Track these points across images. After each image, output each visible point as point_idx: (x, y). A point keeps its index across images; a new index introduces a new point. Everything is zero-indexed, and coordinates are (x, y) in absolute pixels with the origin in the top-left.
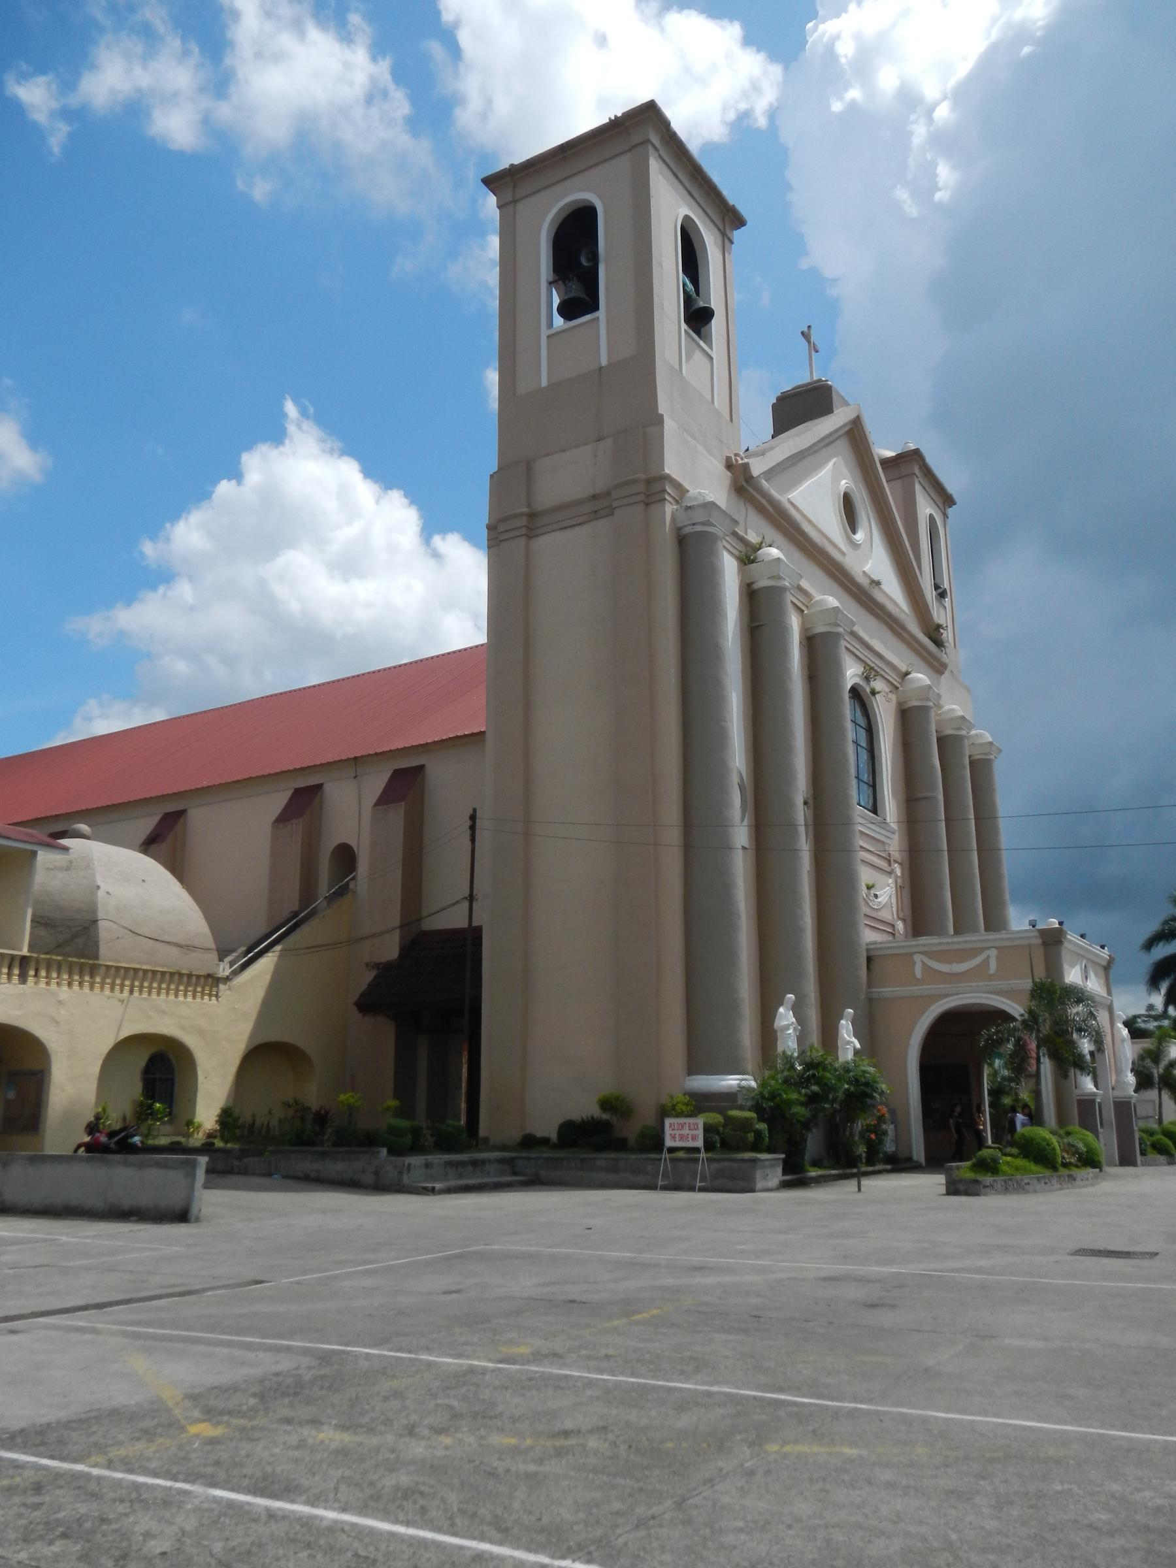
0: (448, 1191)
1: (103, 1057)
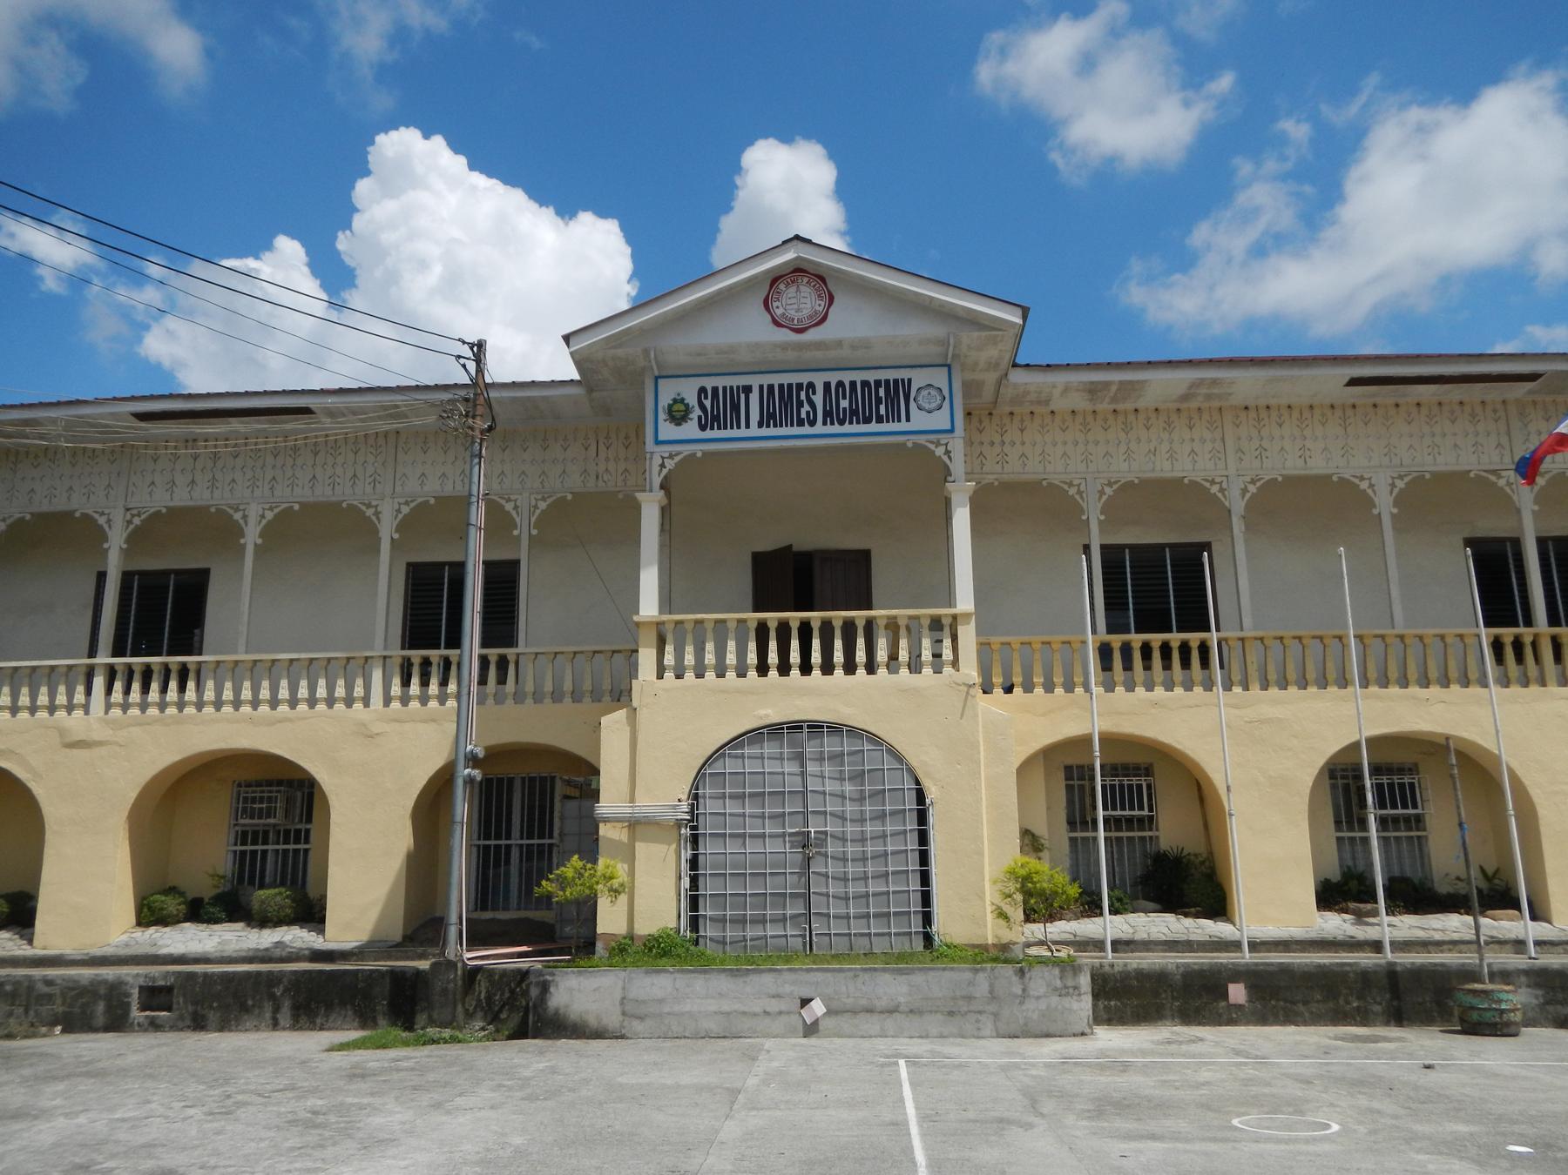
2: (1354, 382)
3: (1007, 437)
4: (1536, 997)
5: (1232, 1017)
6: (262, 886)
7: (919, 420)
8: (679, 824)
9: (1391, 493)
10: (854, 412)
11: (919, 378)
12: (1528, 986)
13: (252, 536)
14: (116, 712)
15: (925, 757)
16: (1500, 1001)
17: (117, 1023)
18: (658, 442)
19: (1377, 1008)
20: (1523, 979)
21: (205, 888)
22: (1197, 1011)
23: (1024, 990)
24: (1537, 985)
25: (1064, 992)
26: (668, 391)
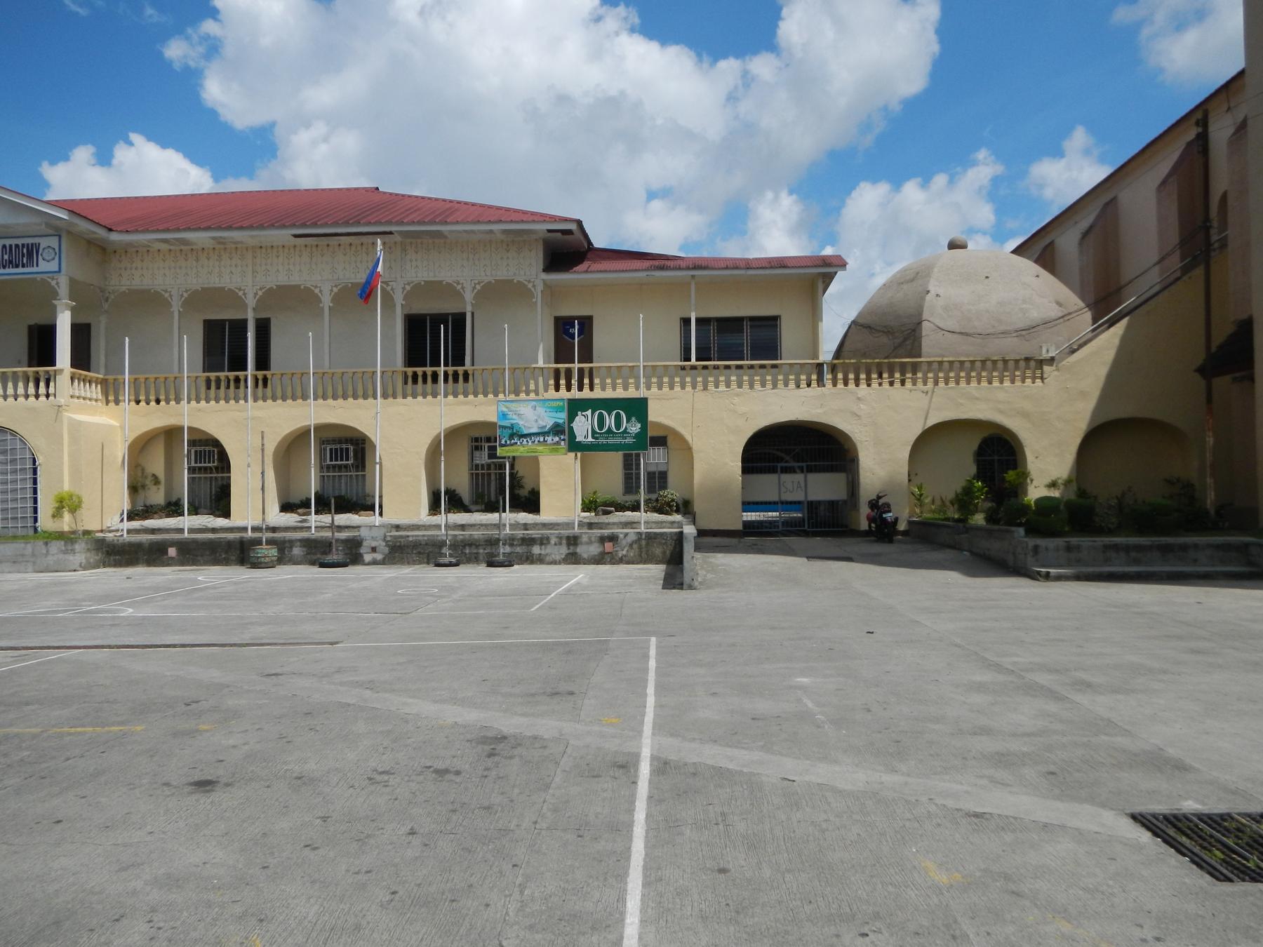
0: (1078, 578)
1: (912, 443)
2: (296, 236)
3: (134, 265)
4: (303, 552)
5: (169, 563)
7: (44, 266)
9: (330, 294)
10: (11, 262)
11: (44, 242)
12: (300, 547)
15: (38, 443)
16: (258, 553)
19: (233, 558)
20: (298, 543)
22: (154, 560)
23: (47, 551)
24: (304, 546)
25: (65, 552)
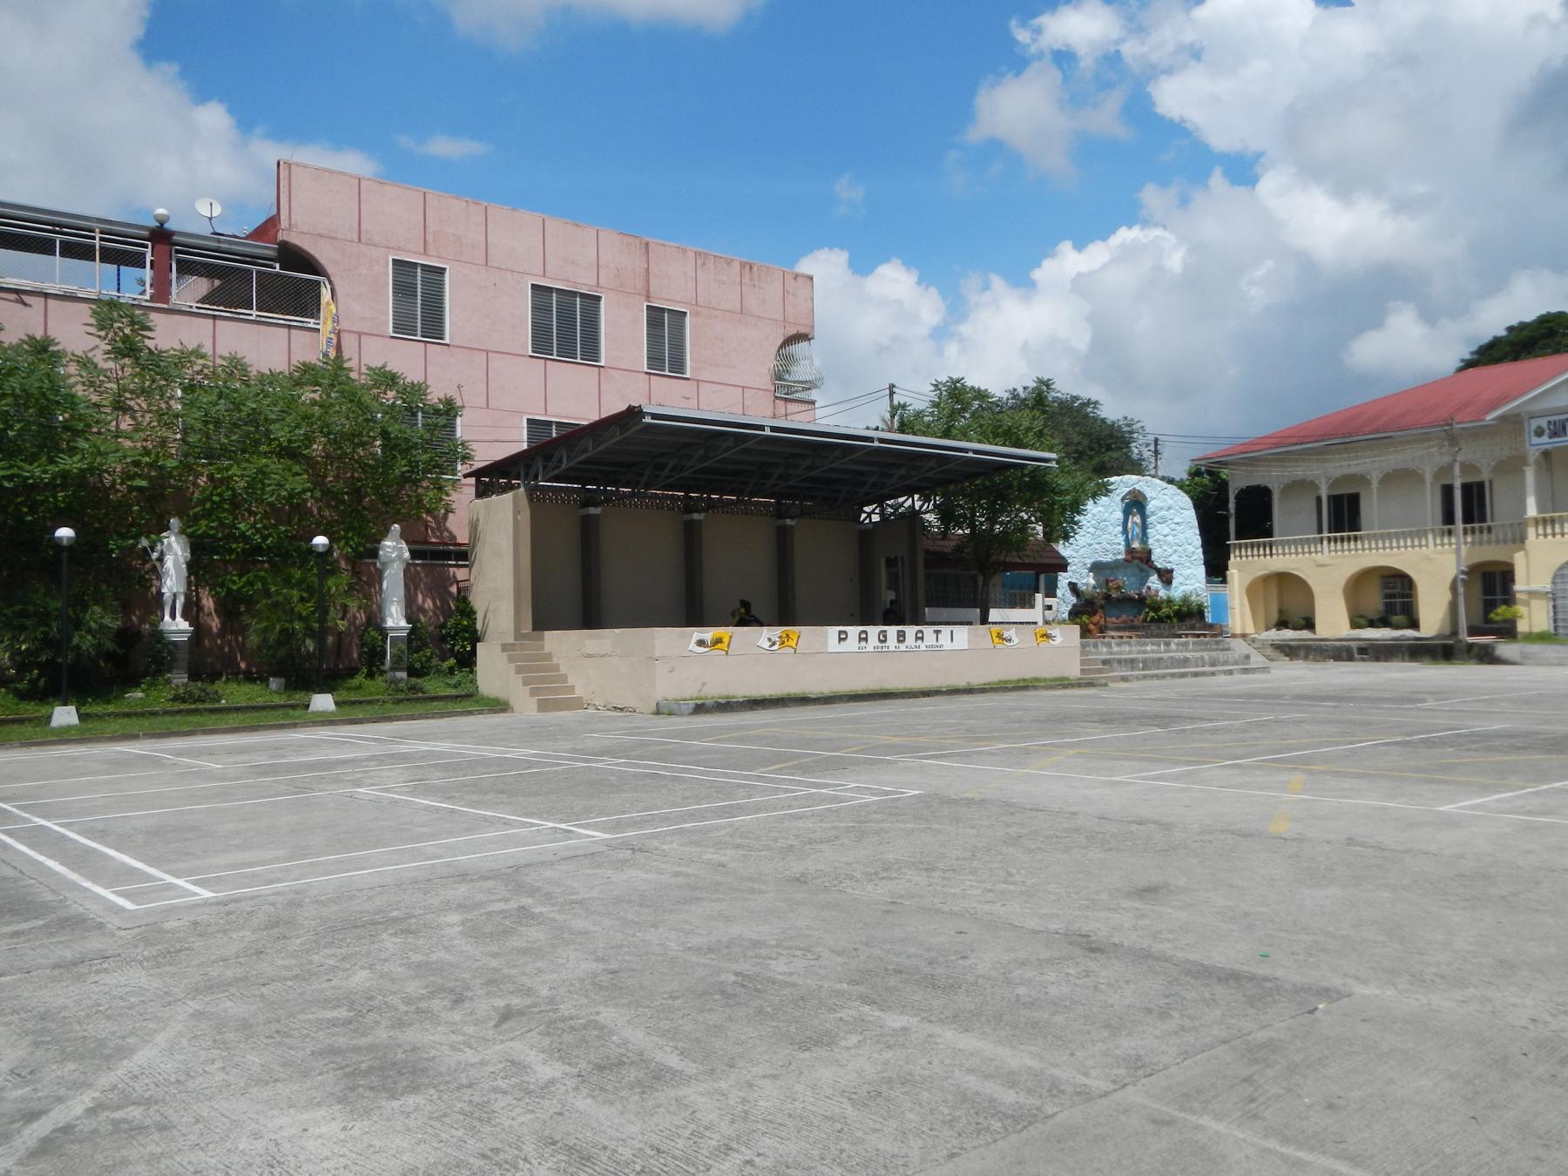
6: (1396, 615)
8: (1548, 593)
13: (1375, 484)
14: (1333, 553)
17: (1350, 658)
18: (1532, 445)
21: (1376, 617)
26: (1535, 424)
